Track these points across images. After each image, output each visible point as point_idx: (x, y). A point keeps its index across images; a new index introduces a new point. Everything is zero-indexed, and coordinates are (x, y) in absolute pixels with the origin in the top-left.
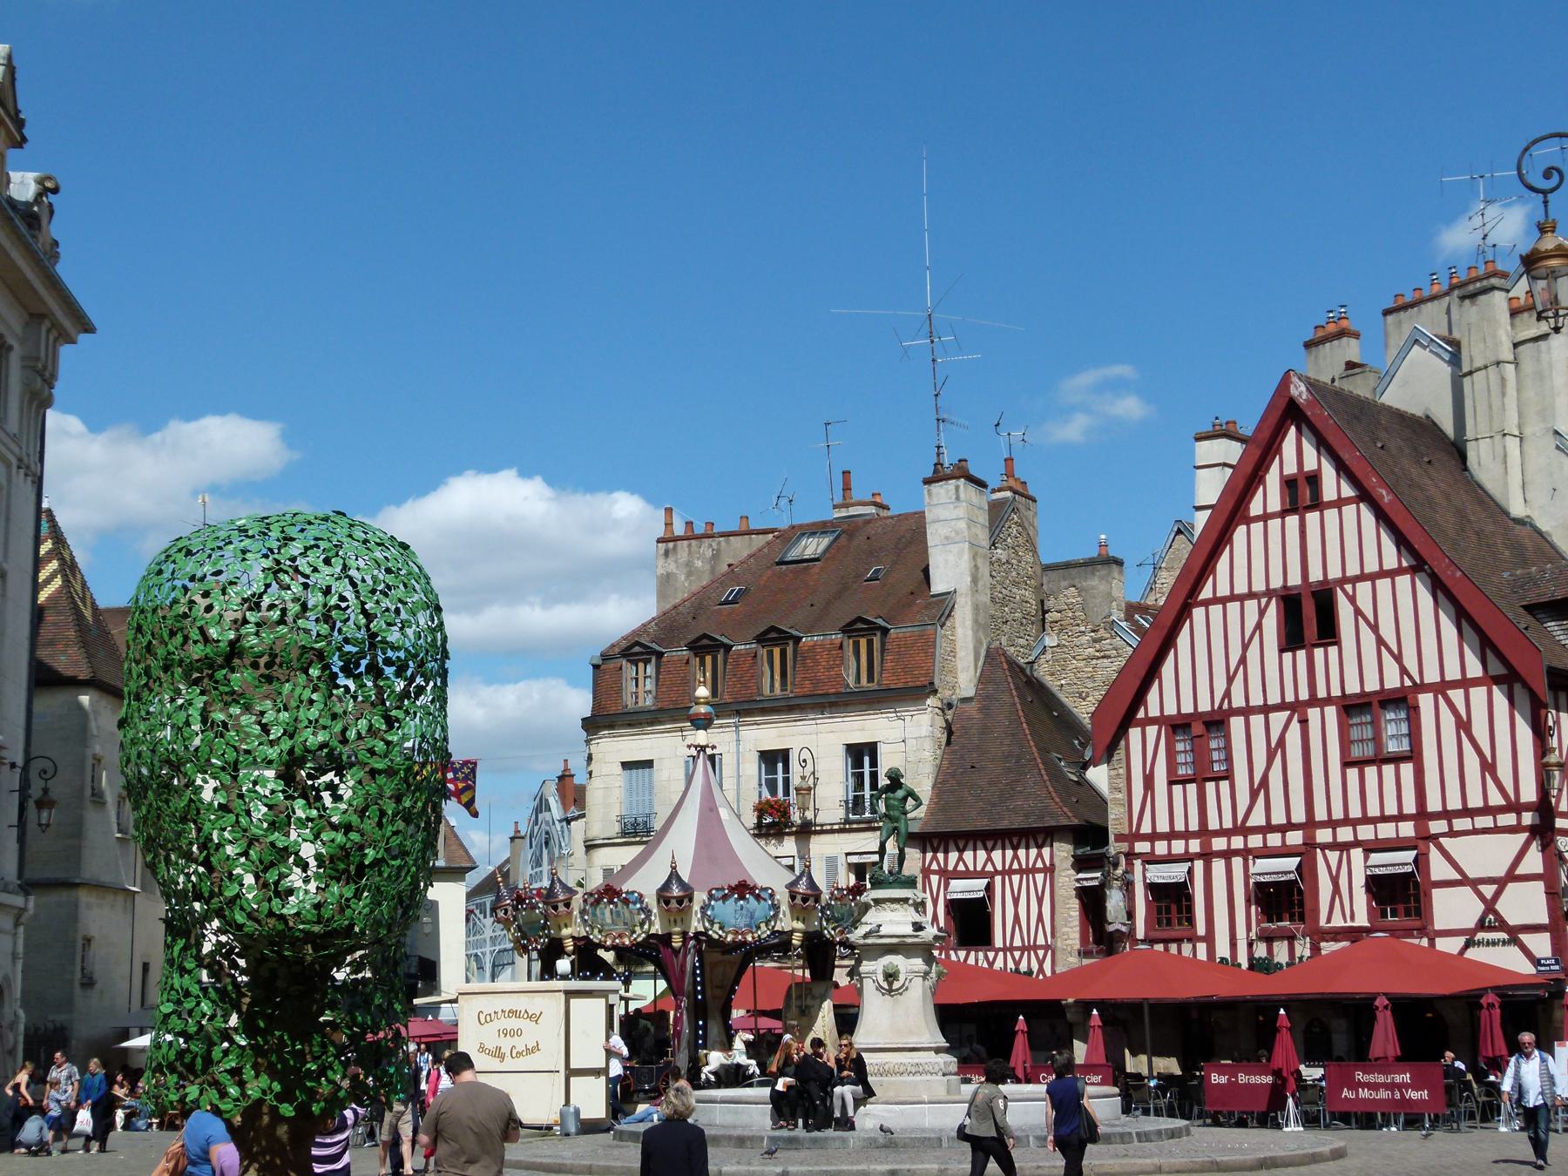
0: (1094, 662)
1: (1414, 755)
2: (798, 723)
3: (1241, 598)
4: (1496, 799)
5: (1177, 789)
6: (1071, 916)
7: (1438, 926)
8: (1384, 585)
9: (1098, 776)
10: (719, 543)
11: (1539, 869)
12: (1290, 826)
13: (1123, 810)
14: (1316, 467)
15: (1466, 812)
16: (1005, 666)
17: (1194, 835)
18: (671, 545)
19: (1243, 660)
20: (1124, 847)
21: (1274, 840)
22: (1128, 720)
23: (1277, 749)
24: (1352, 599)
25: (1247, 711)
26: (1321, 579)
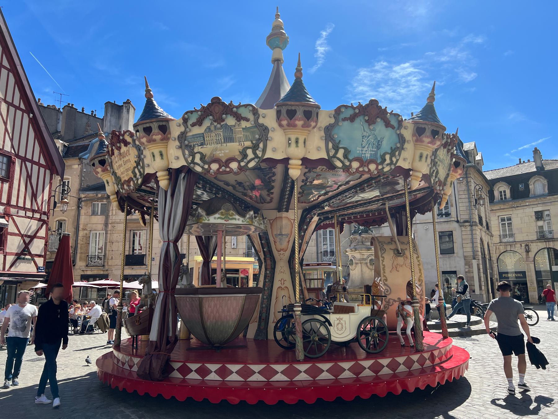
15: (24, 208)
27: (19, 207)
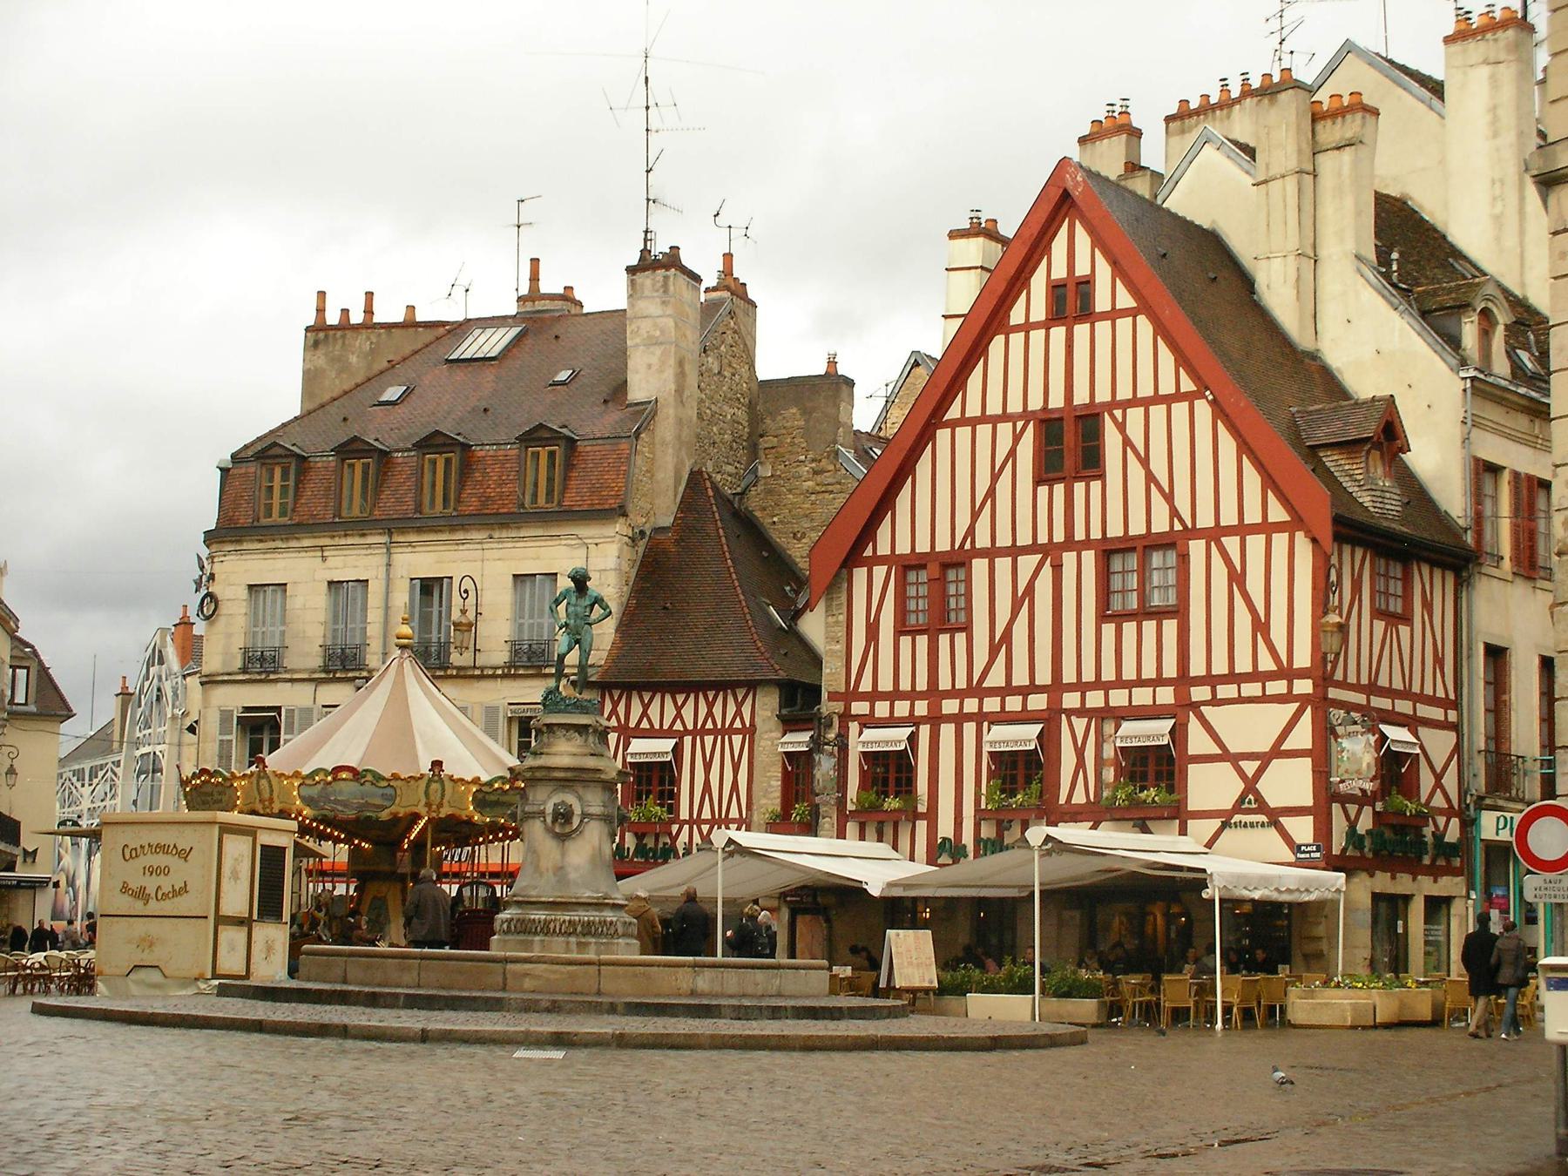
0: (813, 497)
1: (1180, 611)
2: (461, 547)
3: (994, 421)
4: (1266, 664)
5: (905, 641)
6: (770, 786)
7: (1193, 805)
8: (1158, 412)
9: (814, 626)
10: (380, 335)
11: (1307, 744)
12: (1033, 688)
13: (840, 664)
14: (1089, 273)
15: (1233, 677)
16: (710, 493)
17: (921, 696)
18: (321, 335)
19: (991, 493)
20: (838, 707)
21: (1014, 704)
22: (854, 557)
23: (1024, 598)
24: (1122, 427)
25: (992, 553)
26: (1087, 401)
27: (1214, 676)
